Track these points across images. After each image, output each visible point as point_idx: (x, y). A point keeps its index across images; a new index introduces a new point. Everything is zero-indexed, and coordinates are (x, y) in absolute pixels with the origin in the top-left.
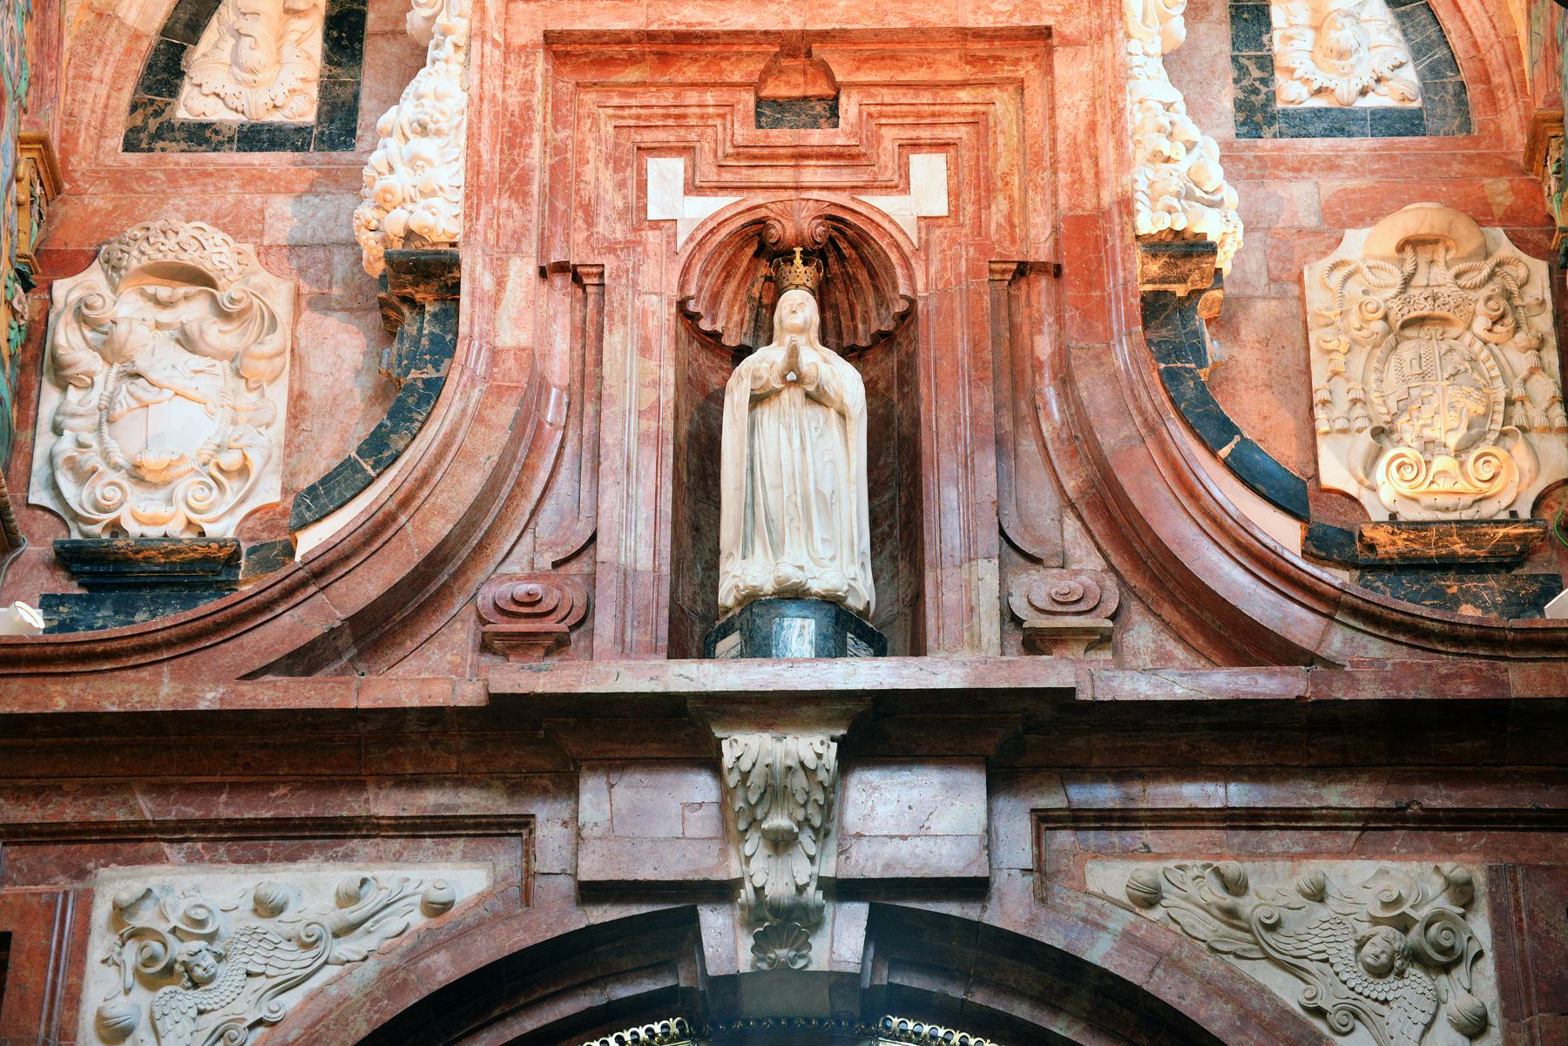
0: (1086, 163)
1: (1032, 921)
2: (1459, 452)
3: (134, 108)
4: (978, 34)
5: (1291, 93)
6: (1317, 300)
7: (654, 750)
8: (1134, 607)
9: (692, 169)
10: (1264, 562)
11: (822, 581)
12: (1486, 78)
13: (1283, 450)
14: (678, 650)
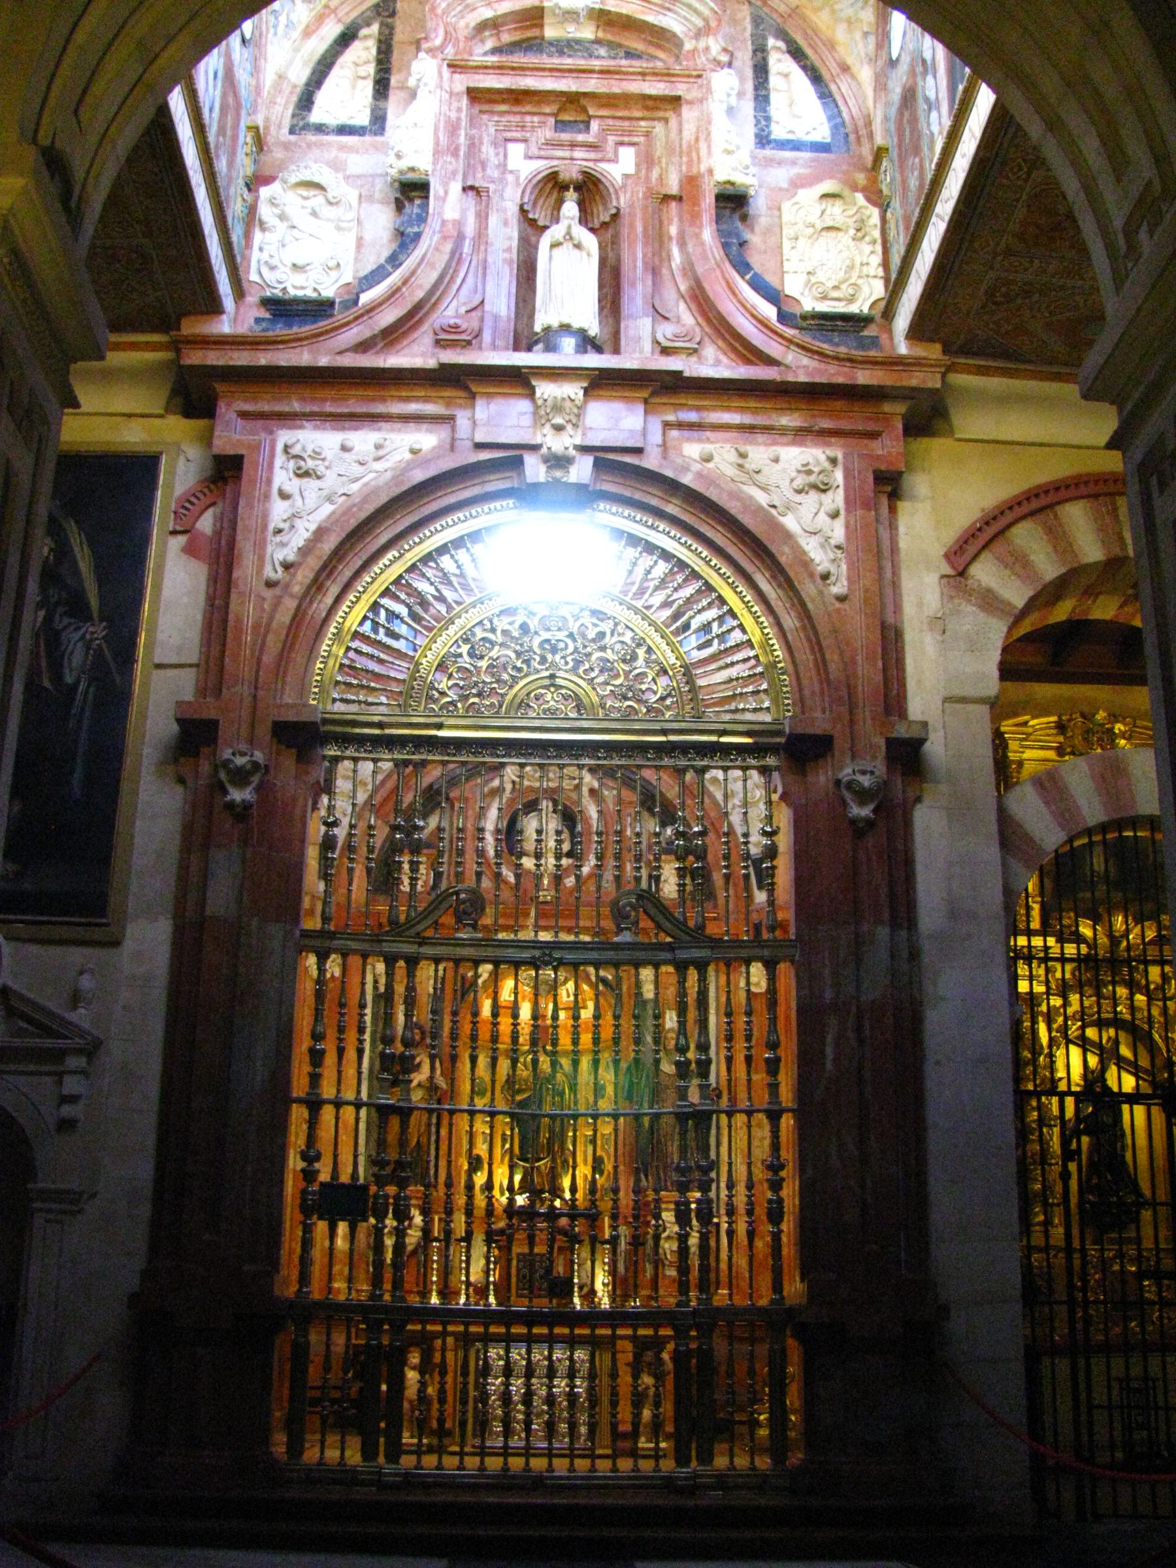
0: (694, 155)
1: (661, 466)
3: (293, 116)
4: (650, 97)
5: (778, 132)
6: (786, 218)
8: (706, 339)
9: (528, 148)
10: (762, 323)
12: (857, 132)
13: (772, 279)
14: (516, 348)
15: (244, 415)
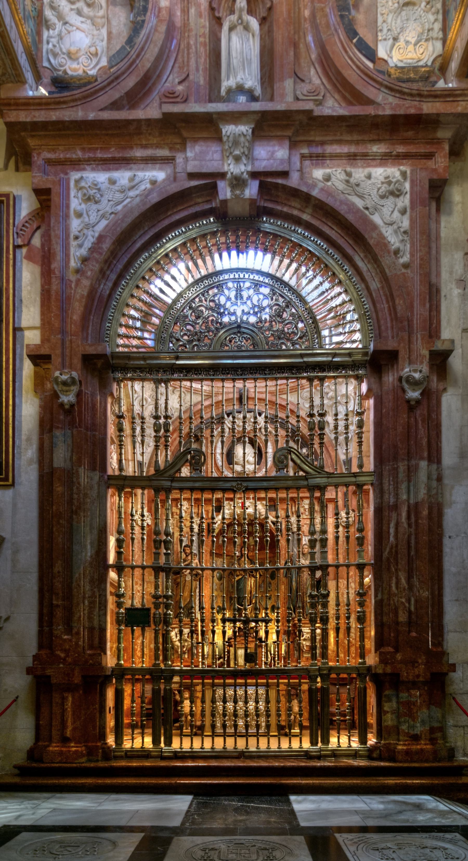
1: (299, 185)
2: (415, 45)
7: (205, 135)
8: (328, 95)
11: (249, 84)
14: (210, 101)
15: (49, 162)
